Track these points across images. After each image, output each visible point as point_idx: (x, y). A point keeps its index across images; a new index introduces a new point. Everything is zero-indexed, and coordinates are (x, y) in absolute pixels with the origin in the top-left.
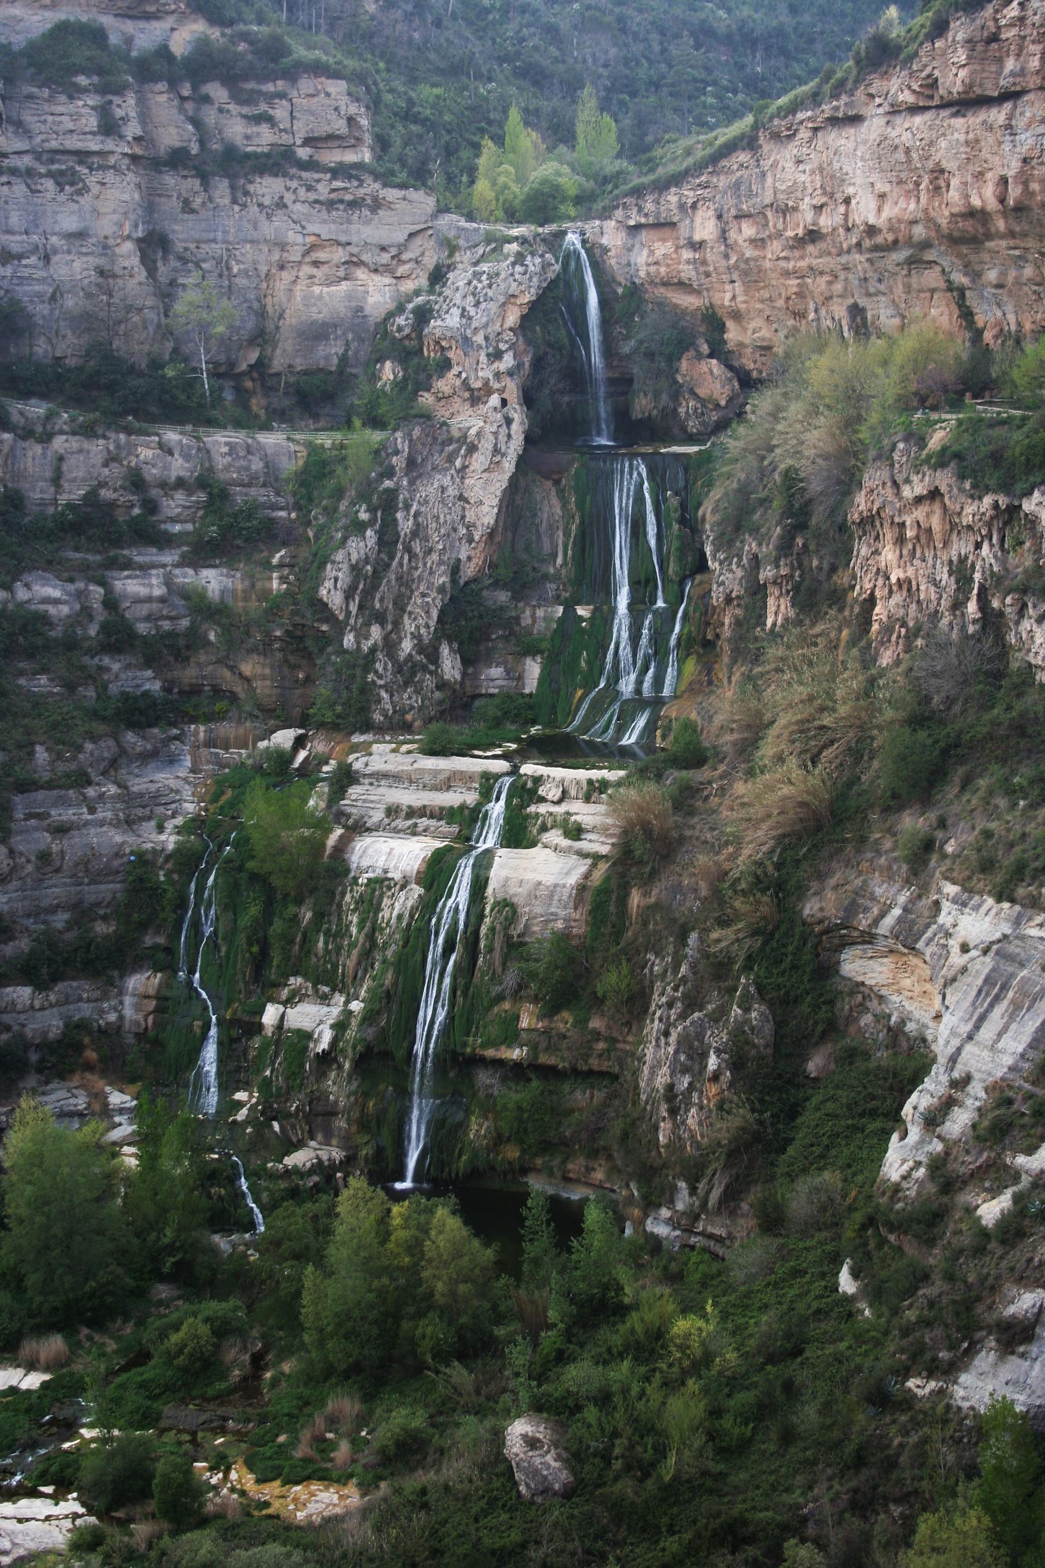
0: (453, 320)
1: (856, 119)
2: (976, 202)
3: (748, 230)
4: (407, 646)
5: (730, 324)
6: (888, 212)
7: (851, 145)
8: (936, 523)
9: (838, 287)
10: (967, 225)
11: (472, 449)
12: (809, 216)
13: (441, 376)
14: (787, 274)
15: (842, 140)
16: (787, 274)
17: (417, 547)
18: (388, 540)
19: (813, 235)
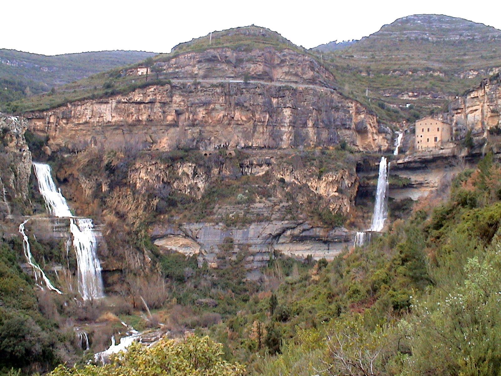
0: (15, 131)
1: (107, 103)
2: (140, 119)
3: (64, 121)
4: (25, 197)
5: (51, 140)
6: (114, 120)
7: (105, 107)
8: (154, 169)
9: (89, 133)
10: (136, 123)
11: (25, 158)
12: (88, 119)
13: (11, 142)
14: (72, 130)
15: (103, 106)
16: (72, 130)
17: (21, 178)
18: (16, 176)
19: (86, 123)
